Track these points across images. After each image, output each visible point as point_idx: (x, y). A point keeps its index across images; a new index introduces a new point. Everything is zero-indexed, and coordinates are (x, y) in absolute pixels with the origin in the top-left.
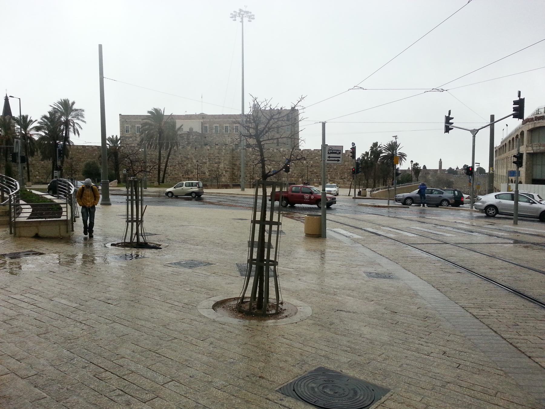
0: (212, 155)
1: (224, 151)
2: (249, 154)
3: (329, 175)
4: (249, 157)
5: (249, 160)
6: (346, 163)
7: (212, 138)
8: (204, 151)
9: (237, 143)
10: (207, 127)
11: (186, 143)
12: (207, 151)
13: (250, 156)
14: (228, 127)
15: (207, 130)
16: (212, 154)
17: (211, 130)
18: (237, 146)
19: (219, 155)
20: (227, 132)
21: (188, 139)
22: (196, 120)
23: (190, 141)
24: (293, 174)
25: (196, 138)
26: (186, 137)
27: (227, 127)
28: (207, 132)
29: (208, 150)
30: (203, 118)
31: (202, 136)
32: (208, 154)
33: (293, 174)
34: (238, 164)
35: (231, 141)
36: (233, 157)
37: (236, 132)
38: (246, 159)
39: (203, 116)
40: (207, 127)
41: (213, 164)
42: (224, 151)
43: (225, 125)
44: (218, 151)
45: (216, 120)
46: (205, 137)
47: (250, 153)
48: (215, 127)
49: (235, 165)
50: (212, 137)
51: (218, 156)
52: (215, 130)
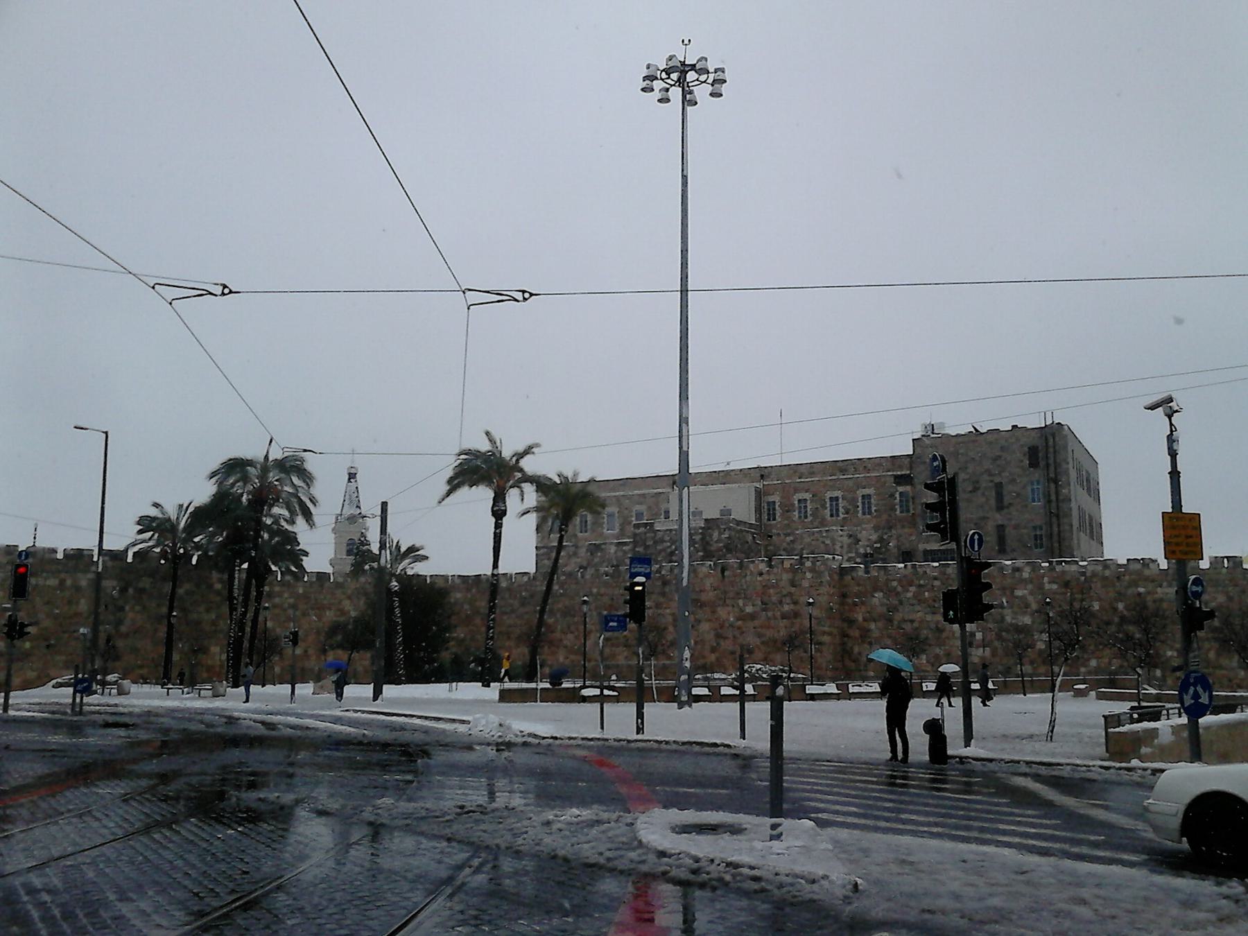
1: (809, 575)
2: (895, 584)
4: (898, 594)
5: (897, 602)
7: (791, 538)
8: (748, 578)
9: (869, 550)
10: (774, 502)
11: (701, 554)
12: (759, 578)
13: (899, 589)
14: (840, 500)
15: (774, 514)
16: (773, 587)
17: (788, 511)
18: (869, 559)
19: (793, 590)
20: (838, 516)
21: (708, 543)
22: (742, 485)
23: (712, 548)
25: (729, 538)
26: (700, 536)
27: (837, 499)
28: (774, 519)
29: (761, 574)
30: (762, 476)
31: (762, 530)
32: (759, 588)
34: (860, 619)
35: (849, 546)
36: (844, 596)
37: (864, 514)
39: (762, 473)
40: (774, 502)
41: (775, 618)
42: (809, 575)
43: (829, 495)
44: (790, 576)
46: (771, 537)
47: (900, 581)
48: (799, 501)
49: (851, 622)
50: (789, 535)
51: (790, 594)
52: (800, 512)
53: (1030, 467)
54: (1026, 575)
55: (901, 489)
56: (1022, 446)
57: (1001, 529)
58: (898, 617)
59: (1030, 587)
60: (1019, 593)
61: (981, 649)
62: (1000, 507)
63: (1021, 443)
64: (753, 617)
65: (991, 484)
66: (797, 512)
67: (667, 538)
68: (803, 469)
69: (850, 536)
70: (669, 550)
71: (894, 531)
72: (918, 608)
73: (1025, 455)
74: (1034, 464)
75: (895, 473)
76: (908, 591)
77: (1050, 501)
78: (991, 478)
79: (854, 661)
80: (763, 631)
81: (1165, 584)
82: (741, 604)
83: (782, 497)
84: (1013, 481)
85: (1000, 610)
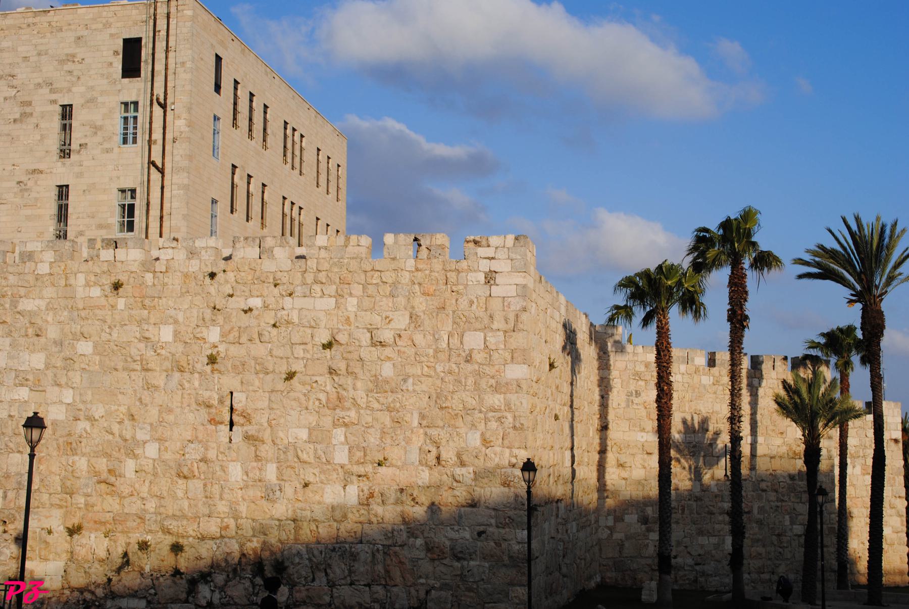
3: (339, 434)
6: (474, 340)
24: (83, 425)
53: (124, 76)
54: (44, 269)
56: (112, 35)
57: (63, 191)
59: (49, 292)
60: (27, 305)
63: (113, 31)
73: (116, 53)
74: (131, 68)
78: (54, 97)
81: (299, 290)
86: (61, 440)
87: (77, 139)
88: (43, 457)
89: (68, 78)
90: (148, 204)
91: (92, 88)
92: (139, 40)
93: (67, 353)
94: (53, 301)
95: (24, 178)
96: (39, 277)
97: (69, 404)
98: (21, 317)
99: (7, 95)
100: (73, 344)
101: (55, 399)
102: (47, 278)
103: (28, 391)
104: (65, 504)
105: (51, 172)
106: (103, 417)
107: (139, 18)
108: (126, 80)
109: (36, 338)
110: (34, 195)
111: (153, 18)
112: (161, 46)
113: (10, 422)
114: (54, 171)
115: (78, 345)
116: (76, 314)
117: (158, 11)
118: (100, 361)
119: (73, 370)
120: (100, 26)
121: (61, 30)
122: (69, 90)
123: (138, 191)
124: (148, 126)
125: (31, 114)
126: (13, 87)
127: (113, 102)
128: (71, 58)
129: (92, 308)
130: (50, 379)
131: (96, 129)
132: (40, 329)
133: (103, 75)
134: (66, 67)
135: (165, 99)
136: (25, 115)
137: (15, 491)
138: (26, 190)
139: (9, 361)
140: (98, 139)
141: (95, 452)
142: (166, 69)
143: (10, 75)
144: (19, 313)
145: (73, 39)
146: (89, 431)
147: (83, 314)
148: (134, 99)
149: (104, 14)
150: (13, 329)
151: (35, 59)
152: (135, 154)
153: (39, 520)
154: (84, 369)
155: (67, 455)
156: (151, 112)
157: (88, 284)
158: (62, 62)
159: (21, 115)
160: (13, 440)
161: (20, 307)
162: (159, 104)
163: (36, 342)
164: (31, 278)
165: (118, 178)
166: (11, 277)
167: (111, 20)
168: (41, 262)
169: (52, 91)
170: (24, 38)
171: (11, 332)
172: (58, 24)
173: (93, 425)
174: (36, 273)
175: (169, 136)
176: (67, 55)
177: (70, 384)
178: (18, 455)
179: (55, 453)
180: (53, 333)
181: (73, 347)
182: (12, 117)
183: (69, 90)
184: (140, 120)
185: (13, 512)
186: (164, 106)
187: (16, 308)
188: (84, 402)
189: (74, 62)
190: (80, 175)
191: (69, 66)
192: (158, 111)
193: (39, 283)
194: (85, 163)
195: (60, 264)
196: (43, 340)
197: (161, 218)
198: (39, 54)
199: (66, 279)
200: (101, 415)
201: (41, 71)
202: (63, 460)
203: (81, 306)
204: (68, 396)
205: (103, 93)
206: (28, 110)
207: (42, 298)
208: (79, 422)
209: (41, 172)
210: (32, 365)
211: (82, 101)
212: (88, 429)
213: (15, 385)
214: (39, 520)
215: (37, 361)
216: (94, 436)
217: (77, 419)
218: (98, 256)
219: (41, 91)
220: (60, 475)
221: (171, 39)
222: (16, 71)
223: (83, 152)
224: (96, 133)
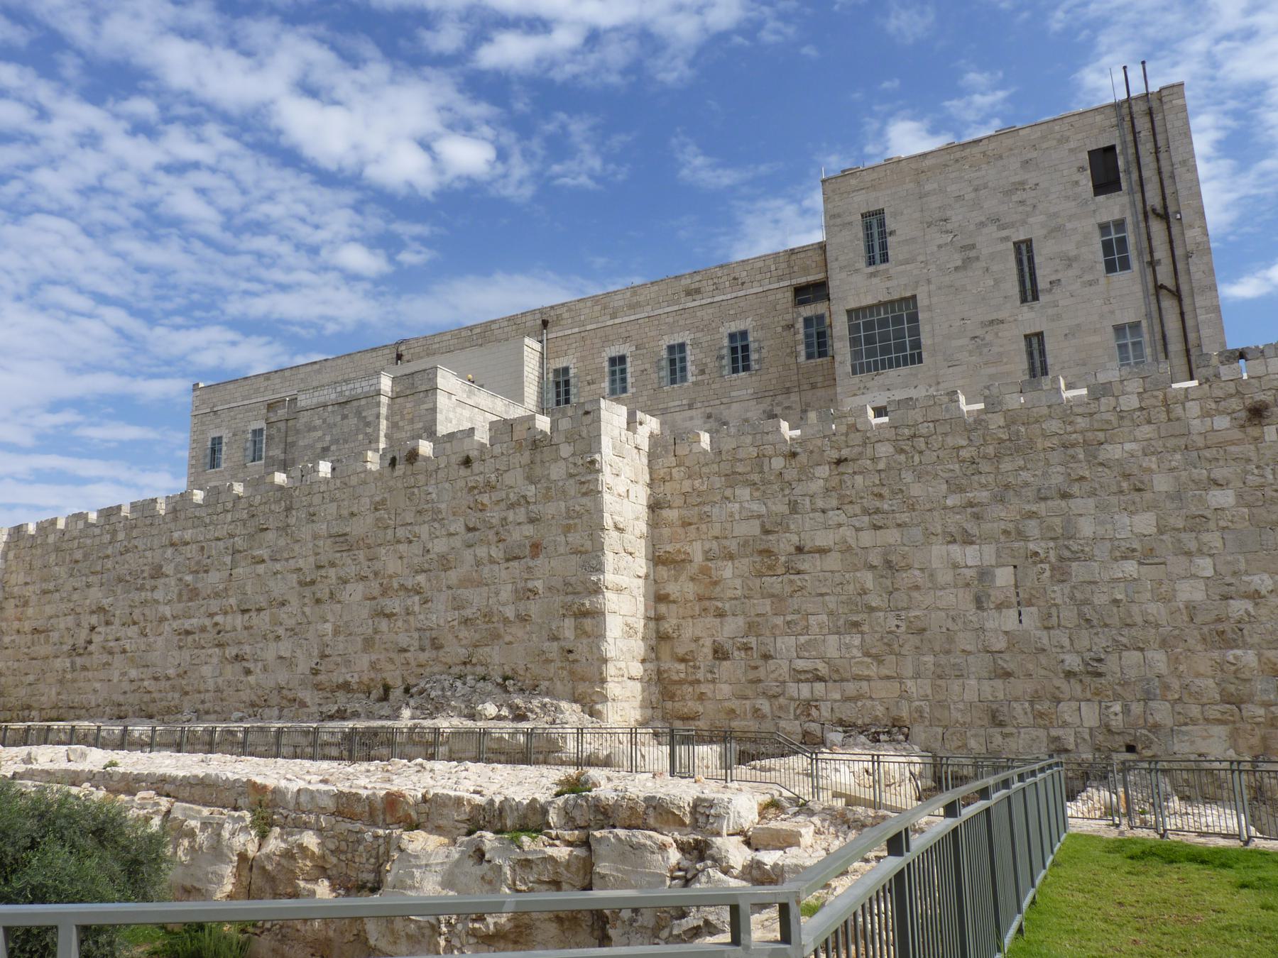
0: (485, 499)
5: (784, 509)
14: (688, 348)
19: (531, 491)
24: (1239, 607)
30: (545, 324)
33: (1249, 605)
38: (756, 507)
41: (492, 561)
42: (566, 450)
45: (617, 321)
54: (1130, 402)
55: (808, 311)
56: (1071, 150)
58: (784, 544)
59: (1146, 431)
60: (1113, 452)
61: (1013, 613)
62: (1029, 291)
63: (1072, 145)
64: (445, 563)
65: (1002, 247)
66: (607, 379)
67: (318, 422)
68: (618, 302)
69: (709, 416)
70: (319, 445)
71: (794, 397)
72: (834, 517)
73: (1081, 169)
75: (794, 282)
76: (813, 478)
77: (1153, 264)
78: (1004, 233)
79: (683, 660)
80: (465, 593)
82: (425, 536)
83: (582, 359)
84: (1056, 231)
85: (1063, 504)
86: (1206, 629)
87: (1044, 276)
88: (1181, 653)
89: (1020, 209)
90: (1164, 337)
91: (1056, 215)
92: (1112, 148)
93: (1194, 510)
94: (1153, 442)
95: (979, 332)
96: (1124, 414)
97: (1208, 578)
98: (1106, 470)
99: (941, 242)
100: (1201, 495)
101: (1183, 573)
102: (1139, 413)
103: (1136, 566)
104: (1231, 718)
105: (1015, 320)
106: (1272, 591)
107: (1107, 123)
108: (1101, 198)
109: (1136, 494)
110: (995, 349)
111: (1128, 118)
112: (1146, 148)
113: (1115, 609)
114: (1020, 318)
115: (1209, 497)
116: (1195, 454)
117: (1135, 109)
118: (1252, 516)
119: (1208, 530)
120: (1055, 143)
121: (1001, 157)
122: (1024, 222)
123: (1144, 324)
124: (1145, 244)
125: (977, 258)
126: (947, 232)
127: (1089, 225)
128: (1020, 186)
129: (1219, 446)
130: (1170, 546)
131: (1069, 261)
132: (1142, 482)
133: (1067, 198)
134: (1015, 198)
135: (1165, 207)
136: (967, 263)
137: (1142, 703)
138: (985, 345)
139: (1098, 528)
140: (1071, 273)
141: (1270, 642)
142: (1160, 173)
143: (942, 220)
144: (1102, 464)
145: (1018, 165)
146: (1253, 613)
147: (1207, 453)
148: (1117, 216)
149: (1057, 128)
150: (1097, 486)
151: (973, 195)
152: (1129, 284)
153: (1193, 742)
154: (1224, 528)
155: (1221, 648)
156: (1147, 227)
157: (1207, 414)
158: (1008, 193)
159: (964, 261)
160: (1125, 631)
161: (1102, 456)
162: (1158, 215)
163: (1138, 499)
164: (1113, 418)
165: (1112, 312)
166: (1079, 419)
167: (1067, 134)
168: (1124, 394)
169: (1002, 227)
170: (952, 176)
171: (1095, 489)
172: (995, 152)
173: (1257, 604)
174: (1118, 409)
175: (1179, 252)
176: (1014, 183)
177: (1205, 550)
178: (1138, 654)
179: (1199, 647)
180: (1162, 483)
181: (1200, 499)
182: (951, 265)
183: (1024, 222)
184: (1131, 240)
185: (1144, 731)
186: (1164, 216)
187: (1095, 458)
188: (1235, 573)
189: (1024, 190)
190: (1058, 317)
191: (1019, 196)
192: (1157, 227)
193: (1126, 422)
194: (1061, 303)
195: (1156, 393)
196: (1148, 496)
197: (1188, 351)
198: (976, 190)
199: (1168, 412)
200: (1270, 588)
201: (982, 207)
202: (1216, 655)
203: (1200, 442)
204: (1205, 566)
205: (1070, 218)
206: (972, 254)
207: (1135, 440)
208: (1231, 601)
209: (1002, 322)
210: (1136, 530)
211: (1044, 232)
212: (1251, 609)
213: (1116, 560)
214: (1193, 742)
215: (1145, 523)
216: (1264, 619)
217: (1226, 598)
218: (1217, 376)
219: (985, 231)
220: (1214, 678)
221: (1159, 137)
222: (949, 213)
223: (1057, 290)
224: (1070, 266)
